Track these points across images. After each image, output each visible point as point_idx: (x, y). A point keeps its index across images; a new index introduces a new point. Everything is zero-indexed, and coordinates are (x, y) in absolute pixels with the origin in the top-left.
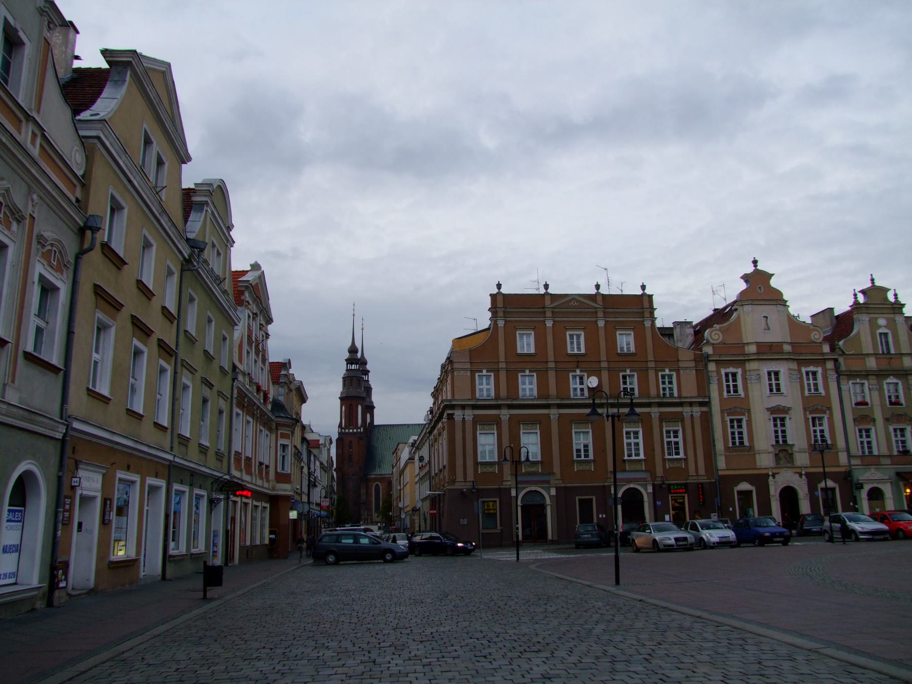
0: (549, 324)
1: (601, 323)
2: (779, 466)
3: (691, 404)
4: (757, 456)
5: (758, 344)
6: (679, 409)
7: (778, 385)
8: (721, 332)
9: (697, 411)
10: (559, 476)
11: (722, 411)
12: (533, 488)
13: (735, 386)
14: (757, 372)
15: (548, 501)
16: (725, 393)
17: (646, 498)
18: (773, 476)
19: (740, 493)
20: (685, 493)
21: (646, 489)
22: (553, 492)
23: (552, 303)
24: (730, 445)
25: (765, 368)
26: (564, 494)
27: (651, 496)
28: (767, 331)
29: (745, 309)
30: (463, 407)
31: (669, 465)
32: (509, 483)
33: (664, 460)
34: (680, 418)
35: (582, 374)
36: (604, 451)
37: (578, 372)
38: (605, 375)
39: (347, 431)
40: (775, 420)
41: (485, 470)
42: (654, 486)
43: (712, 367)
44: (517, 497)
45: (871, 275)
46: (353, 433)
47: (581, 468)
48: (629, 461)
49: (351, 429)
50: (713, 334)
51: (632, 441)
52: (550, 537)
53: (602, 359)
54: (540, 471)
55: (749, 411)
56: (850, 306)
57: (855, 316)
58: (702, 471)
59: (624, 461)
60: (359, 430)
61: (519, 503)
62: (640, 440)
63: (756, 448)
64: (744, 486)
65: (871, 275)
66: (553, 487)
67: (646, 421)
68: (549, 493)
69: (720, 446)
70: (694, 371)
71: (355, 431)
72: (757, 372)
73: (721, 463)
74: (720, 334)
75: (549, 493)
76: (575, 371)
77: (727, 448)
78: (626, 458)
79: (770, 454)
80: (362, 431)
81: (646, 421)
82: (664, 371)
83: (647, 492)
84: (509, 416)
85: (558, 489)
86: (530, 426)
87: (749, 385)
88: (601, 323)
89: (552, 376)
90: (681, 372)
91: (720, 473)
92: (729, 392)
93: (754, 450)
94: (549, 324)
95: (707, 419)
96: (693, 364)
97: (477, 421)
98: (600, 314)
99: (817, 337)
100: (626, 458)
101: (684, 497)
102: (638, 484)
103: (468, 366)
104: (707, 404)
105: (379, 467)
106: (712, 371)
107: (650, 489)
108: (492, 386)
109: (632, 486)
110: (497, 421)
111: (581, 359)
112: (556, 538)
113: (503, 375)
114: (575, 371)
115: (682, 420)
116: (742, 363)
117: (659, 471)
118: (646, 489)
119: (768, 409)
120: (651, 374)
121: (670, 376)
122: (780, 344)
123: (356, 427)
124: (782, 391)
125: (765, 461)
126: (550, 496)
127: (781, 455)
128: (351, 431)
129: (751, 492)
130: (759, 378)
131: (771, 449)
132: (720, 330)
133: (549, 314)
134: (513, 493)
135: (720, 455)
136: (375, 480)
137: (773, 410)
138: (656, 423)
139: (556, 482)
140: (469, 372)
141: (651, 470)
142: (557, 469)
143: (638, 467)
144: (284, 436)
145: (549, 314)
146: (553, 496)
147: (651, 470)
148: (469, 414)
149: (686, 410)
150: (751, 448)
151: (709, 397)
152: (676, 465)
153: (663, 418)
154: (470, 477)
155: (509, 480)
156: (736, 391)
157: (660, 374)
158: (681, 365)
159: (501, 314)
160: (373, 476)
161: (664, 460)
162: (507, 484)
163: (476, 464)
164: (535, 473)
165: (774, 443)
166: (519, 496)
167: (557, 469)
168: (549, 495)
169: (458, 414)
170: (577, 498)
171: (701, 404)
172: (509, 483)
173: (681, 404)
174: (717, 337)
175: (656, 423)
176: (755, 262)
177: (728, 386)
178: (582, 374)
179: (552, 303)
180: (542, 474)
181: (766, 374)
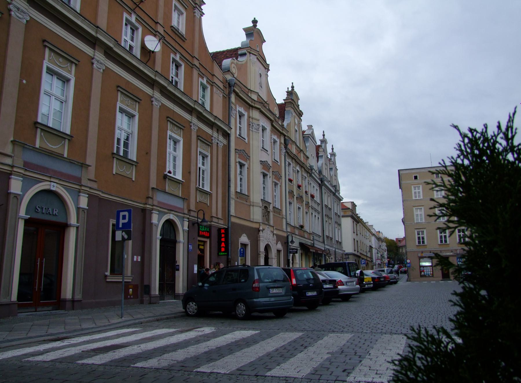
4: (252, 207)
12: (55, 187)
15: (73, 220)
20: (207, 237)
22: (84, 202)
27: (186, 234)
29: (251, 58)
31: (199, 198)
32: (8, 161)
35: (137, 25)
36: (148, 153)
37: (133, 19)
44: (18, 198)
45: (292, 83)
54: (66, 156)
56: (284, 100)
57: (286, 109)
61: (22, 213)
64: (244, 239)
65: (292, 83)
66: (85, 192)
68: (77, 202)
75: (77, 202)
84: (28, 19)
85: (91, 197)
86: (61, 60)
87: (251, 132)
101: (205, 242)
102: (177, 216)
118: (183, 226)
126: (78, 209)
139: (90, 184)
146: (83, 209)
164: (56, 156)
176: (255, 22)
178: (137, 25)
180: (70, 161)
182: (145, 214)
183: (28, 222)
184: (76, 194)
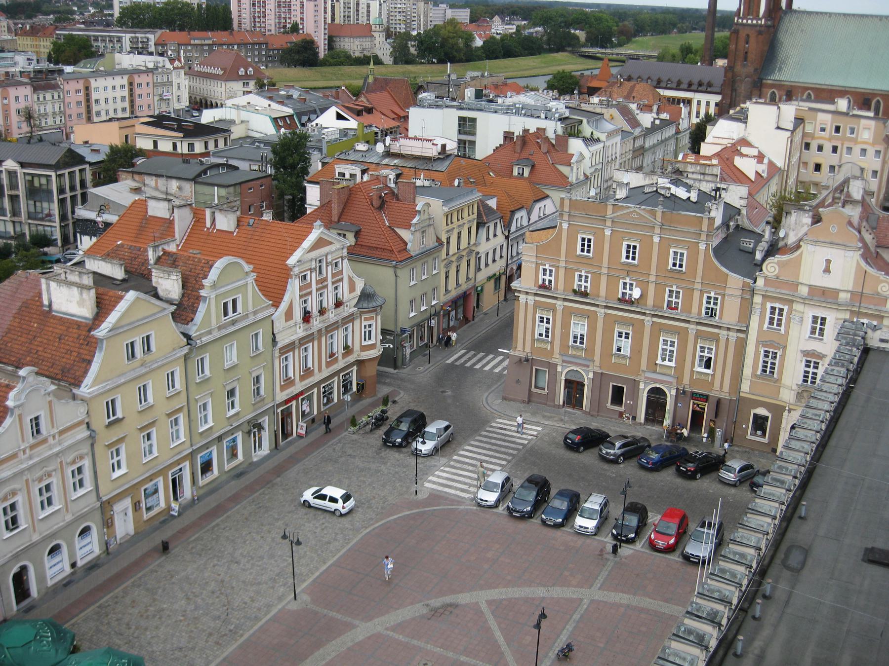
0: (608, 232)
1: (656, 239)
2: (799, 404)
3: (729, 329)
5: (812, 288)
6: (716, 331)
7: (821, 330)
8: (779, 266)
9: (733, 336)
10: (597, 363)
11: (758, 342)
12: (575, 368)
13: (780, 320)
14: (801, 315)
15: (586, 383)
16: (766, 325)
17: (668, 399)
18: (790, 411)
19: (755, 415)
21: (670, 392)
22: (591, 375)
23: (613, 213)
24: (759, 372)
25: (809, 313)
26: (600, 378)
27: (674, 398)
28: (826, 275)
30: (527, 293)
32: (557, 360)
33: (692, 372)
34: (716, 339)
36: (640, 352)
38: (652, 288)
39: (745, 21)
40: (807, 361)
41: (540, 346)
42: (677, 389)
43: (758, 299)
44: (562, 373)
46: (752, 26)
47: (617, 361)
48: (660, 365)
49: (750, 19)
50: (769, 266)
51: (669, 348)
52: (584, 409)
53: (651, 273)
55: (785, 347)
58: (726, 388)
59: (656, 364)
60: (759, 22)
61: (563, 378)
62: (675, 349)
63: (783, 381)
64: (762, 411)
67: (682, 334)
68: (587, 375)
69: (747, 371)
70: (739, 300)
71: (754, 22)
72: (801, 315)
73: (745, 387)
74: (777, 267)
75: (587, 375)
76: (625, 279)
77: (754, 375)
78: (659, 361)
79: (793, 392)
80: (763, 23)
81: (682, 334)
82: (710, 293)
83: (671, 394)
88: (656, 239)
89: (604, 281)
90: (726, 298)
91: (741, 394)
92: (771, 323)
93: (780, 383)
94: (608, 232)
95: (741, 346)
96: (740, 292)
97: (537, 305)
98: (657, 230)
99: (884, 289)
100: (659, 361)
103: (534, 260)
104: (746, 332)
105: (780, 69)
106: (756, 303)
107: (674, 392)
108: (553, 278)
109: (658, 386)
110: (553, 309)
111: (632, 269)
112: (588, 410)
113: (562, 272)
114: (625, 279)
115: (718, 341)
116: (790, 302)
117: (686, 380)
118: (670, 392)
119: (802, 352)
120: (696, 294)
121: (716, 299)
122: (836, 292)
123: (757, 17)
124: (825, 337)
125: (787, 396)
127: (805, 394)
128: (750, 22)
129: (767, 418)
130: (802, 320)
131: (795, 387)
132: (778, 263)
133: (609, 223)
134: (559, 369)
135: (746, 379)
136: (772, 86)
137: (805, 353)
138: (691, 337)
140: (534, 265)
141: (679, 379)
142: (597, 357)
143: (668, 372)
144: (366, 319)
145: (609, 223)
147: (679, 379)
148: (531, 299)
149: (723, 333)
150: (778, 380)
151: (748, 327)
152: (703, 377)
153: (699, 335)
154: (528, 349)
155: (556, 359)
156: (779, 325)
157: (705, 295)
158: (727, 291)
159: (566, 217)
160: (769, 82)
161: (692, 372)
162: (553, 361)
163: (533, 340)
165: (800, 382)
166: (563, 372)
167: (597, 357)
168: (587, 378)
169: (522, 297)
170: (611, 384)
171: (739, 331)
172: (557, 360)
173: (719, 327)
174: (773, 269)
175: (691, 337)
177: (772, 319)
179: (613, 213)
180: (585, 359)
181: (811, 320)
182: (636, 383)
183: (566, 380)
184: (587, 372)
